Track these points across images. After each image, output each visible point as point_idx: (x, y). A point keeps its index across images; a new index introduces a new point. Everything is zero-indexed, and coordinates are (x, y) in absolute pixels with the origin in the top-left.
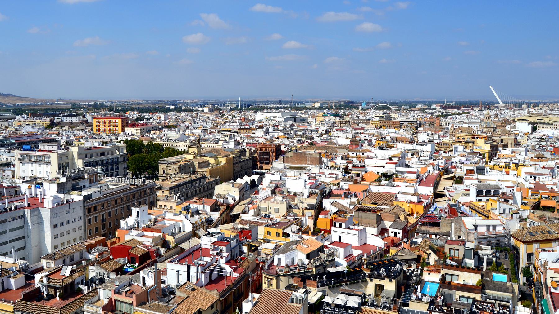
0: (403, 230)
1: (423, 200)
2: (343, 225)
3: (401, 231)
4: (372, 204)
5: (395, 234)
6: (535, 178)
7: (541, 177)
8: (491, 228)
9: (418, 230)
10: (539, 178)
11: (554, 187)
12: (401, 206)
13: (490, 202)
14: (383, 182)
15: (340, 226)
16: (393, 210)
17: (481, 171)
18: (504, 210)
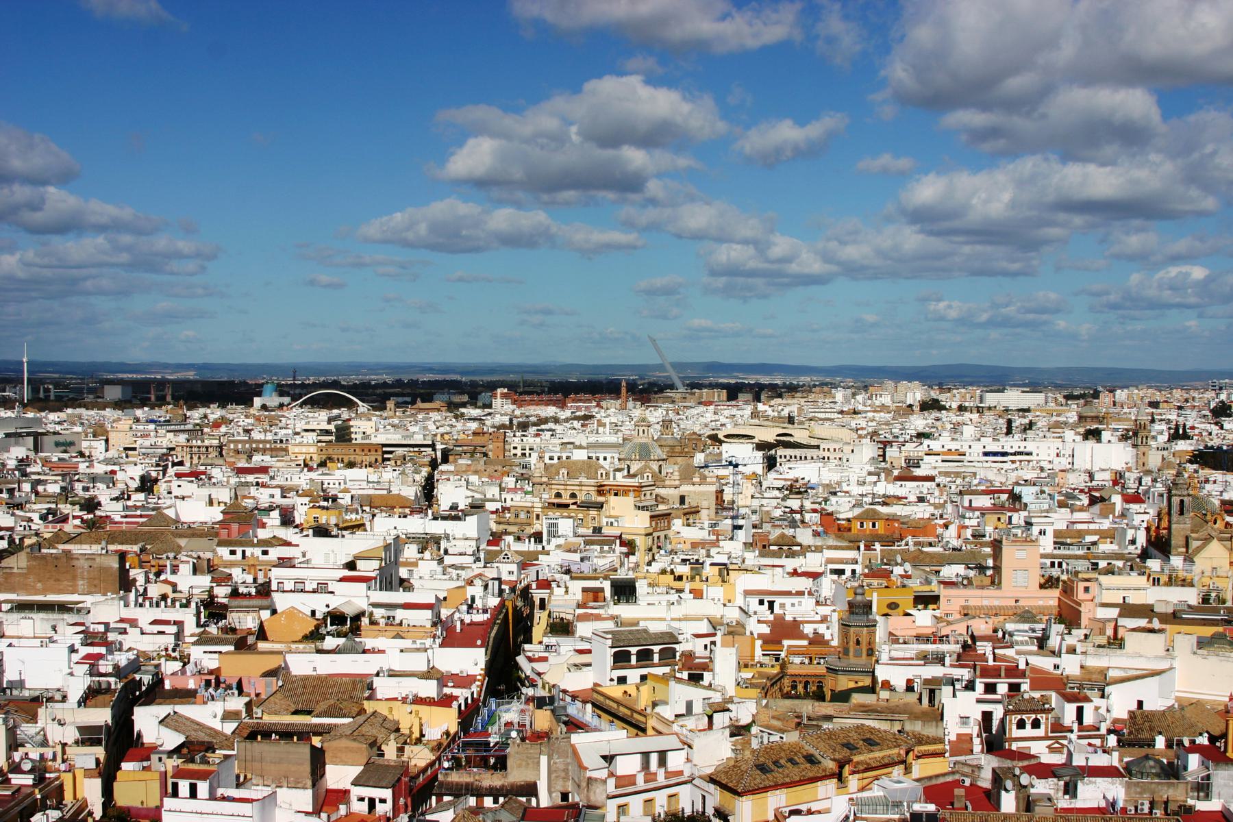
0: (393, 787)
1: (456, 692)
2: (203, 788)
3: (387, 794)
4: (296, 713)
5: (372, 803)
6: (771, 604)
7: (788, 601)
8: (654, 758)
9: (441, 783)
10: (782, 606)
11: (822, 629)
12: (385, 712)
13: (650, 682)
14: (330, 642)
15: (193, 794)
16: (364, 729)
17: (625, 591)
18: (689, 705)
